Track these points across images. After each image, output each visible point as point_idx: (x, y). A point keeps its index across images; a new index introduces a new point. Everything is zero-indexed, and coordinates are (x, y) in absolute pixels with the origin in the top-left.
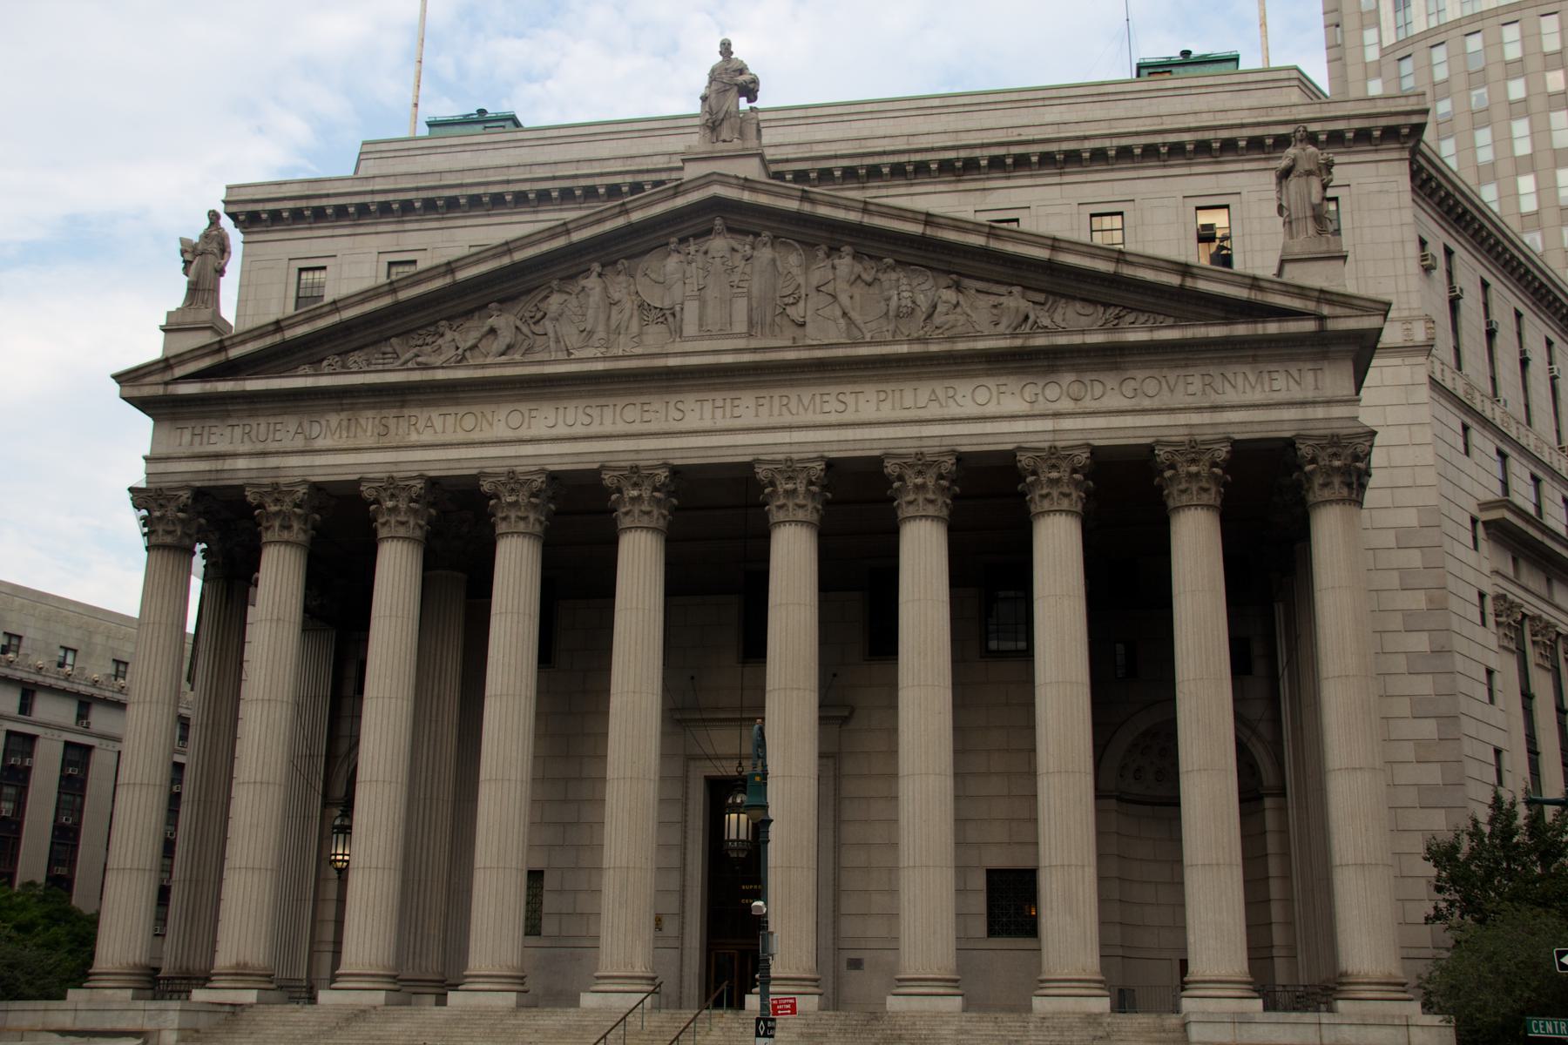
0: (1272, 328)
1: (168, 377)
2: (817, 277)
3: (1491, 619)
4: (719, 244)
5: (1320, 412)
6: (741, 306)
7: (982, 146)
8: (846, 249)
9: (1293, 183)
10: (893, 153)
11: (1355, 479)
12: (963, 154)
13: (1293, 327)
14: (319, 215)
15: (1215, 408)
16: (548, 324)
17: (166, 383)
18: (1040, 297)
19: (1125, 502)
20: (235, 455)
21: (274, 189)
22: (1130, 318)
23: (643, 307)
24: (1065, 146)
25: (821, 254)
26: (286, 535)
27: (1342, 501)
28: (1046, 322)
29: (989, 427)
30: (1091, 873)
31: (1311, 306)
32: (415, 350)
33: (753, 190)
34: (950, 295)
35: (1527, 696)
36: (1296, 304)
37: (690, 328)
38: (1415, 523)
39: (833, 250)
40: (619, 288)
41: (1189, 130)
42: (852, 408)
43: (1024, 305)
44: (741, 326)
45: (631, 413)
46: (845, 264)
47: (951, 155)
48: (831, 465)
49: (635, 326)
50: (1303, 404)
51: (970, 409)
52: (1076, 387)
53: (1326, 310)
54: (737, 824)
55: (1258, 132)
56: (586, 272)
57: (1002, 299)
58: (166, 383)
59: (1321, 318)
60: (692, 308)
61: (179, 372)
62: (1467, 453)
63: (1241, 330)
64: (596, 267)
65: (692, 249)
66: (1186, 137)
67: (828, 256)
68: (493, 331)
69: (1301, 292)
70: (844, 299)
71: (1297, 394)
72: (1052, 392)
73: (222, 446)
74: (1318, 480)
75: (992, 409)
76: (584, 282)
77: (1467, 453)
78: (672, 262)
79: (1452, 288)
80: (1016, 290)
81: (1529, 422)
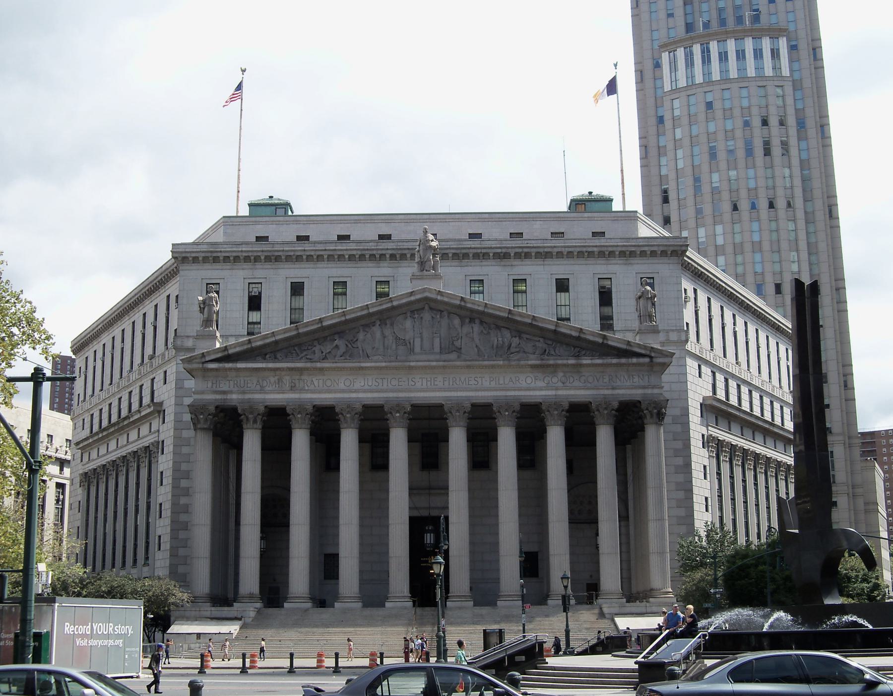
0: (634, 360)
1: (203, 360)
2: (466, 329)
3: (706, 445)
4: (427, 315)
5: (649, 391)
6: (437, 342)
7: (512, 248)
8: (477, 321)
9: (642, 301)
10: (474, 248)
11: (660, 416)
12: (504, 251)
13: (642, 360)
14: (216, 260)
15: (613, 388)
16: (359, 344)
17: (203, 363)
18: (550, 342)
19: (579, 423)
20: (231, 392)
21: (195, 246)
22: (583, 352)
23: (397, 339)
24: (546, 250)
25: (467, 320)
26: (255, 426)
27: (656, 423)
28: (553, 353)
29: (531, 393)
30: (568, 557)
31: (648, 353)
32: (305, 353)
33: (442, 296)
34: (516, 341)
35: (719, 474)
36: (643, 352)
37: (417, 349)
38: (679, 414)
39: (472, 320)
40: (388, 332)
41: (596, 246)
42: (480, 383)
43: (545, 346)
44: (437, 349)
45: (394, 382)
46: (477, 327)
47: (499, 251)
48: (474, 405)
49: (394, 347)
50: (644, 387)
51: (524, 384)
52: (563, 379)
53: (653, 355)
54: (429, 538)
55: (624, 249)
56: (374, 324)
57: (537, 343)
58: (203, 363)
59: (651, 357)
60: (418, 342)
61: (207, 359)
62: (700, 376)
63: (623, 360)
64: (378, 323)
65: (416, 316)
66: (595, 249)
67: (470, 322)
68: (337, 346)
69: (645, 347)
70: (477, 341)
71: (642, 383)
72: (555, 380)
73: (226, 388)
74: (648, 417)
75: (533, 385)
76: (374, 328)
77: (700, 376)
78: (408, 323)
79: (696, 307)
80: (541, 340)
81: (725, 356)
